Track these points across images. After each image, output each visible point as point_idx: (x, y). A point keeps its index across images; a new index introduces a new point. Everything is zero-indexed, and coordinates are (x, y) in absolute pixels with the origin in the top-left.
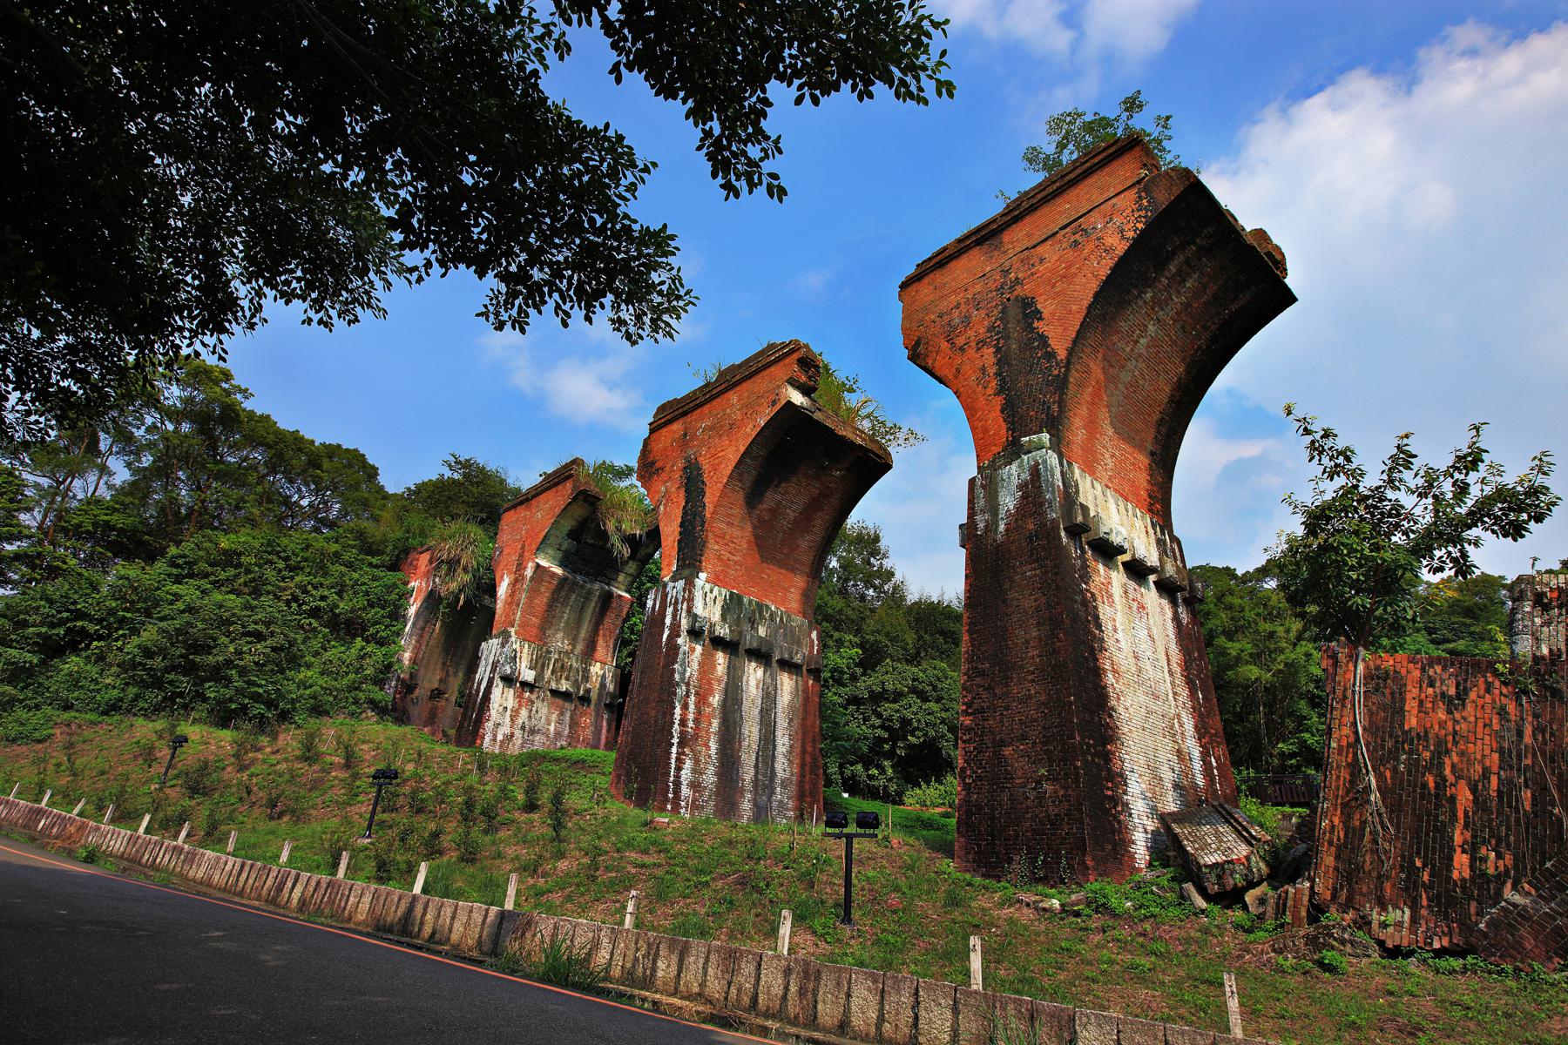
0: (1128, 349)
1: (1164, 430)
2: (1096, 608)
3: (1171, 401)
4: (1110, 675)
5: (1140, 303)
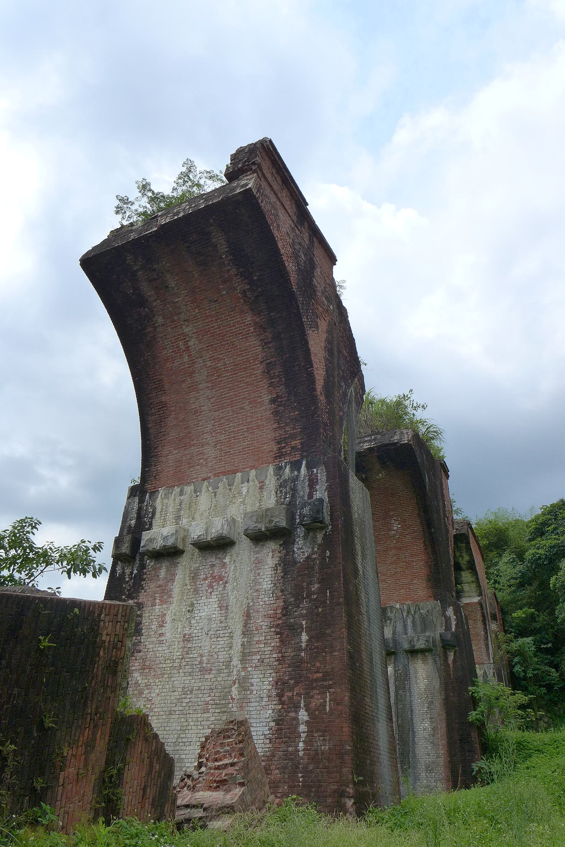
0: (186, 359)
1: (277, 370)
2: (140, 616)
3: (265, 344)
4: (136, 675)
5: (160, 329)
